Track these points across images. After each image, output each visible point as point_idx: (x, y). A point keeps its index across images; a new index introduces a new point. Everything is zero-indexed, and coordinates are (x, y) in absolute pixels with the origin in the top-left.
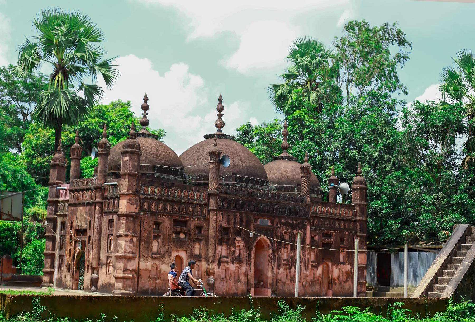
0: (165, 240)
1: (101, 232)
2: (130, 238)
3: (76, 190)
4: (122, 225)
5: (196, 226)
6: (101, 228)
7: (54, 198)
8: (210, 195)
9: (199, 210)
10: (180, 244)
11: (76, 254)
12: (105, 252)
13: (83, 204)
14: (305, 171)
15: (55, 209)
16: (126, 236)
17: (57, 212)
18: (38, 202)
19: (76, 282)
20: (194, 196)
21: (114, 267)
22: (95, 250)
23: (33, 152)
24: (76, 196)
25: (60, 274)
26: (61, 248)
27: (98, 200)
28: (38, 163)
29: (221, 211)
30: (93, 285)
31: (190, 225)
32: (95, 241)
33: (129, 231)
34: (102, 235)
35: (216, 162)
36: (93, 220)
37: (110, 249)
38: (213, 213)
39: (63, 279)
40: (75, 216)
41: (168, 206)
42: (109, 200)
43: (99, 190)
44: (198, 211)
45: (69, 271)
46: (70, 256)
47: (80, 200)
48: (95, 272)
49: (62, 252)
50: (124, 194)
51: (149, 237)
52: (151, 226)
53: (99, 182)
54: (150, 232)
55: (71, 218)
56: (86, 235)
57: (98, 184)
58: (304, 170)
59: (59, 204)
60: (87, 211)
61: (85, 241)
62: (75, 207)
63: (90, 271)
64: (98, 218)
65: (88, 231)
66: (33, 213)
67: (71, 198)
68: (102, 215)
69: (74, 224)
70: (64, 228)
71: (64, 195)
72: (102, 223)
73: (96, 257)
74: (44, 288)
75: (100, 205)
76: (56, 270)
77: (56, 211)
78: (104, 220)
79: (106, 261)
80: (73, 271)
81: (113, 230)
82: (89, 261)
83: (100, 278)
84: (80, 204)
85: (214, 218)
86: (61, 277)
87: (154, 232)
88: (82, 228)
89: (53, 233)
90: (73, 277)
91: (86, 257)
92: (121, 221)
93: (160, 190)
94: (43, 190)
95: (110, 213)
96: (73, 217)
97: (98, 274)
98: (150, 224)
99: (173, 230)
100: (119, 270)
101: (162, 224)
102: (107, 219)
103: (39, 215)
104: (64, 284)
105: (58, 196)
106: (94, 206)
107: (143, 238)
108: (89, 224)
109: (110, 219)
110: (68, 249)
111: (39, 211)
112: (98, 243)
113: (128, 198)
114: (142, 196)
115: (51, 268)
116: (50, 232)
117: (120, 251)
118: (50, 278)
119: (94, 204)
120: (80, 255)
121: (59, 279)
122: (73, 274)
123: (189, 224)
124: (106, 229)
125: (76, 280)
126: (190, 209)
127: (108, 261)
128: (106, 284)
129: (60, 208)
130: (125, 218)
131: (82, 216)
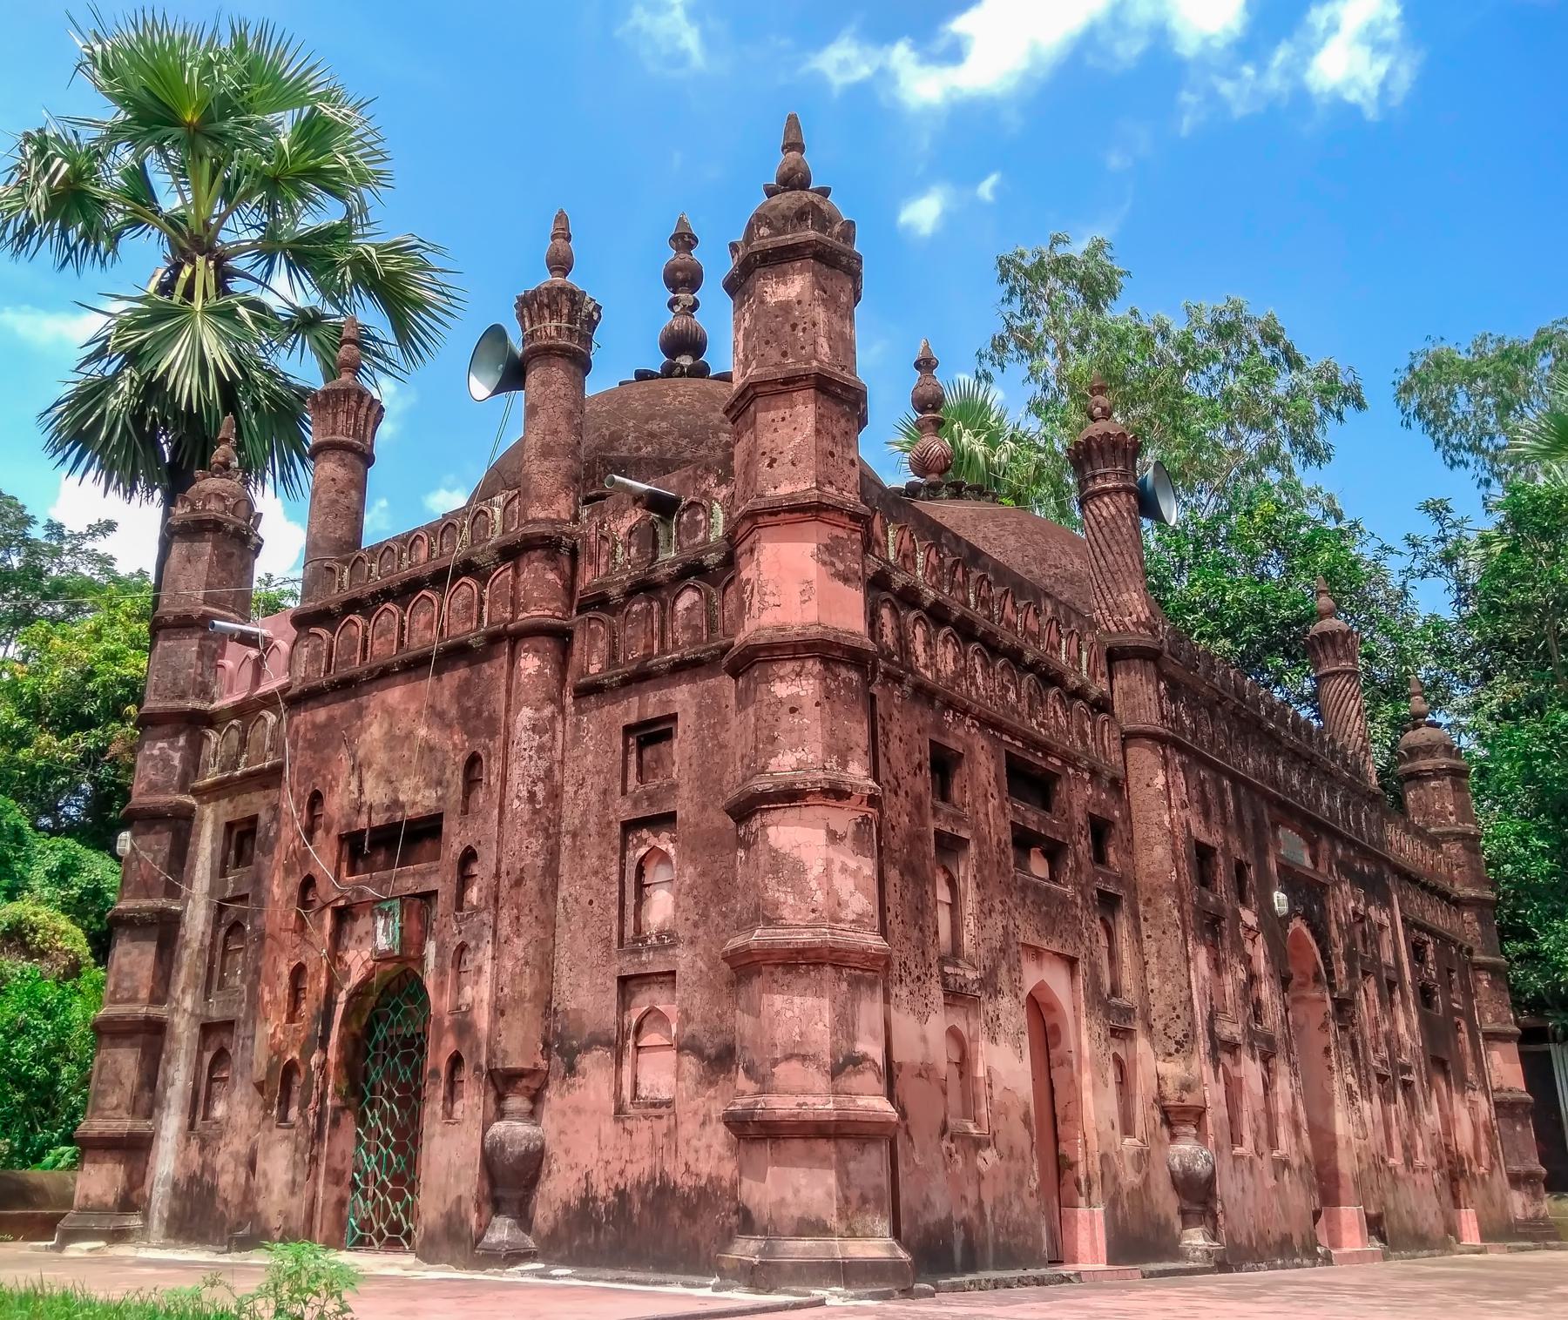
0: (986, 872)
1: (557, 821)
2: (857, 815)
3: (352, 605)
4: (788, 721)
5: (1091, 816)
6: (555, 795)
7: (182, 696)
8: (1116, 656)
9: (1088, 726)
10: (1047, 913)
11: (342, 997)
12: (598, 951)
13: (415, 666)
14: (1341, 653)
15: (183, 760)
16: (836, 793)
18: (31, 891)
19: (336, 1192)
20: (1060, 643)
21: (698, 1051)
22: (519, 944)
23: (19, 723)
24: (352, 639)
25: (202, 1149)
26: (211, 982)
27: (532, 614)
28: (38, 757)
29: (1180, 747)
30: (497, 1210)
31: (1070, 803)
33: (844, 764)
34: (567, 840)
35: (1128, 491)
36: (500, 740)
37: (638, 929)
38: (1154, 751)
39: (225, 1180)
40: (343, 754)
41: (979, 670)
42: (614, 610)
44: (1085, 732)
45: (284, 1117)
46: (291, 1019)
47: (383, 649)
48: (516, 1102)
49: (228, 1003)
50: (791, 510)
51: (916, 838)
52: (920, 766)
53: (537, 512)
54: (918, 804)
55: (307, 773)
56: (437, 857)
57: (535, 521)
58: (1333, 645)
59: (211, 733)
60: (445, 700)
61: (430, 896)
62: (345, 699)
63: (472, 1100)
64: (534, 728)
65: (450, 826)
66: (9, 925)
67: (314, 657)
68: (562, 710)
69: (336, 804)
70: (242, 858)
71: (248, 671)
72: (562, 762)
73: (528, 991)
74: (78, 1249)
75: (547, 643)
76: (171, 1124)
78: (577, 741)
79: (613, 1014)
80: (320, 1116)
81: (674, 786)
82: (464, 1027)
83: (553, 1148)
84: (383, 675)
85: (1160, 781)
86: (204, 1167)
87: (936, 810)
88: (398, 816)
90: (314, 1160)
91: (440, 1003)
92: (781, 690)
93: (934, 560)
94: (52, 849)
95: (641, 677)
96: (325, 762)
97: (533, 1115)
98: (917, 757)
99: (1011, 817)
101: (965, 768)
102: (606, 729)
103: (35, 931)
104: (233, 1215)
105: (204, 692)
106: (504, 659)
107: (896, 843)
108: (458, 779)
110: (285, 970)
111: (35, 914)
112: (542, 892)
113: (826, 531)
114: (873, 565)
115: (133, 1111)
116: (146, 889)
118: (129, 1177)
119: (508, 639)
120: (372, 999)
121: (193, 1179)
122: (317, 1136)
123: (1063, 796)
124: (605, 792)
125: (336, 1177)
126: (1058, 708)
127: (633, 1017)
129: (222, 750)
130: (813, 666)
131: (393, 741)
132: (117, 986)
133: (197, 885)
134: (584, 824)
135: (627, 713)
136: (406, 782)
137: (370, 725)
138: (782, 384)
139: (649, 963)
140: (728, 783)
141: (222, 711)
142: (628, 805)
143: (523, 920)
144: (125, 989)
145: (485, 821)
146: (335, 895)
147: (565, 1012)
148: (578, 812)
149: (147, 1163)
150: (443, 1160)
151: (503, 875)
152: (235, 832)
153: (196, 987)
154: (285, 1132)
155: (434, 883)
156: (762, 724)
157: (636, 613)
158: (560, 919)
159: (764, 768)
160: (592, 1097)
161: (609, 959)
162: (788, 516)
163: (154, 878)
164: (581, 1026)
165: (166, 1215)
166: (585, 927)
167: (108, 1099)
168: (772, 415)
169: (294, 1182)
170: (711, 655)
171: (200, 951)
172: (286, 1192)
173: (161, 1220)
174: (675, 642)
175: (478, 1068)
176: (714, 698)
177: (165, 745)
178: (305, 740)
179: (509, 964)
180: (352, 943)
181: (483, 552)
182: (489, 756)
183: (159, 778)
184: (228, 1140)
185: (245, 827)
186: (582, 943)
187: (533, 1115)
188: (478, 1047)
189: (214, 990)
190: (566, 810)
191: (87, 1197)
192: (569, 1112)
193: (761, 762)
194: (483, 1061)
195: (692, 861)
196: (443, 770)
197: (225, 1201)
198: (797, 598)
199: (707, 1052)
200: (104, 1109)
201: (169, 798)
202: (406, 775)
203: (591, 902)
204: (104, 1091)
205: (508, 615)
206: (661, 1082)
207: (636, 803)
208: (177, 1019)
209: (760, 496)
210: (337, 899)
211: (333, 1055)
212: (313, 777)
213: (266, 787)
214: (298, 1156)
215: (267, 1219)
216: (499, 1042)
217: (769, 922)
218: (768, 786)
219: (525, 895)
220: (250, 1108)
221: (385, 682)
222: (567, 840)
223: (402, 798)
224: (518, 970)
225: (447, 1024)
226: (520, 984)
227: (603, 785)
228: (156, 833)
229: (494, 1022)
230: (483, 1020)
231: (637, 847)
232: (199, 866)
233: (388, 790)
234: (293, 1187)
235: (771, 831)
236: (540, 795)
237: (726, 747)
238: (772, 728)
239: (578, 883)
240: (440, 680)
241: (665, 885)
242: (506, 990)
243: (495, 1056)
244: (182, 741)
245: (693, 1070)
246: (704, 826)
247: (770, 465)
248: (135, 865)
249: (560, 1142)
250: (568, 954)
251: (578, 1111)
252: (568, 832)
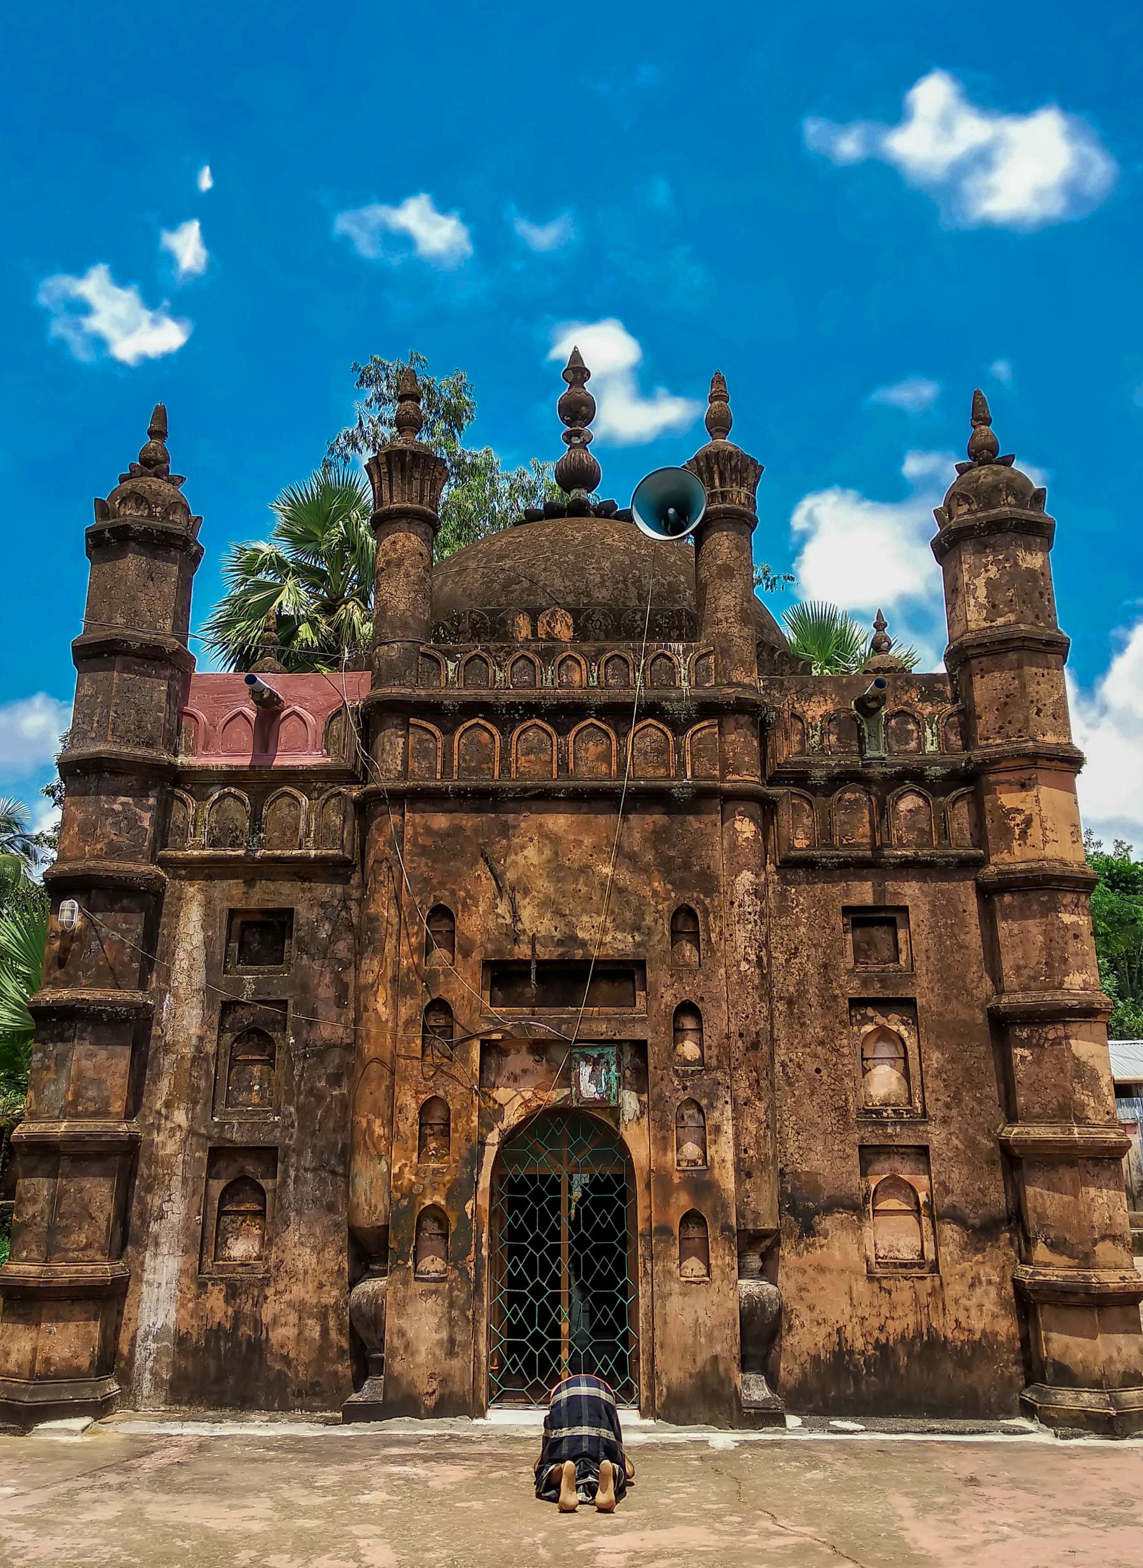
7: (149, 745)
11: (493, 1137)
12: (830, 1119)
17: (164, 846)
27: (748, 778)
32: (755, 1046)
39: (282, 1334)
42: (814, 789)
43: (745, 719)
57: (739, 684)
62: (480, 811)
77: (163, 834)
88: (579, 954)
89: (143, 985)
92: (1067, 918)
100: (1108, 1243)
102: (822, 905)
108: (665, 927)
109: (854, 902)
116: (112, 976)
117: (1090, 1113)
121: (215, 1333)
124: (825, 966)
128: (877, 1345)
132: (78, 1095)
133: (179, 979)
134: (802, 993)
135: (847, 893)
136: (585, 918)
137: (523, 847)
138: (1044, 645)
139: (896, 1135)
140: (973, 981)
141: (205, 771)
142: (856, 983)
143: (763, 1084)
144: (90, 1100)
145: (708, 978)
146: (486, 1027)
147: (795, 1173)
148: (792, 980)
149: (120, 1313)
150: (688, 1318)
151: (735, 1037)
152: (238, 921)
153: (195, 1102)
154: (433, 1286)
155: (639, 1032)
156: (1054, 944)
157: (849, 800)
158: (780, 1081)
159: (1062, 983)
160: (838, 1255)
161: (847, 1126)
162: (1059, 764)
163: (123, 964)
164: (817, 1189)
165: (166, 1376)
166: (812, 1093)
167: (74, 1237)
168: (1034, 670)
169: (452, 1341)
170: (948, 863)
171: (194, 1059)
172: (440, 1353)
173: (157, 1383)
174: (900, 839)
175: (726, 1228)
176: (949, 900)
177: (130, 800)
178: (415, 844)
179: (753, 1127)
180: (502, 1080)
181: (679, 700)
182: (706, 913)
183: (124, 840)
184: (281, 1287)
185: (248, 918)
186: (810, 1109)
187: (767, 1273)
188: (725, 1207)
189: (220, 1107)
190: (778, 976)
191: (47, 1361)
192: (810, 1271)
193: (1057, 979)
194: (733, 1221)
195: (938, 1047)
196: (640, 913)
197: (286, 1359)
198: (1069, 838)
199: (971, 1221)
200: (67, 1250)
201: (143, 868)
202: (584, 911)
203: (818, 1071)
204: (67, 1227)
205: (717, 773)
206: (901, 1243)
207: (865, 983)
208: (158, 1138)
209: (1035, 740)
210: (490, 1032)
211: (484, 1201)
212: (433, 889)
213: (304, 880)
214: (455, 1313)
215: (412, 1383)
216: (748, 1204)
217: (1081, 1121)
218: (1075, 1002)
219: (762, 1059)
220: (319, 1250)
221: (542, 804)
222: (782, 1006)
223: (581, 934)
224: (761, 1132)
225: (676, 1180)
226: (765, 1147)
227: (821, 959)
228: (123, 910)
229: (739, 1182)
230: (728, 1180)
231: (862, 1023)
232: (181, 954)
233: (558, 920)
234: (451, 1347)
235: (1072, 1041)
236: (765, 959)
237: (967, 948)
238: (1063, 950)
239: (800, 1050)
240: (625, 819)
241: (887, 1061)
242: (751, 1152)
243: (744, 1217)
244: (152, 801)
245: (956, 1236)
246: (948, 1016)
247: (1037, 714)
248: (95, 944)
249: (801, 1298)
250: (794, 1118)
251: (821, 1269)
252: (781, 998)
